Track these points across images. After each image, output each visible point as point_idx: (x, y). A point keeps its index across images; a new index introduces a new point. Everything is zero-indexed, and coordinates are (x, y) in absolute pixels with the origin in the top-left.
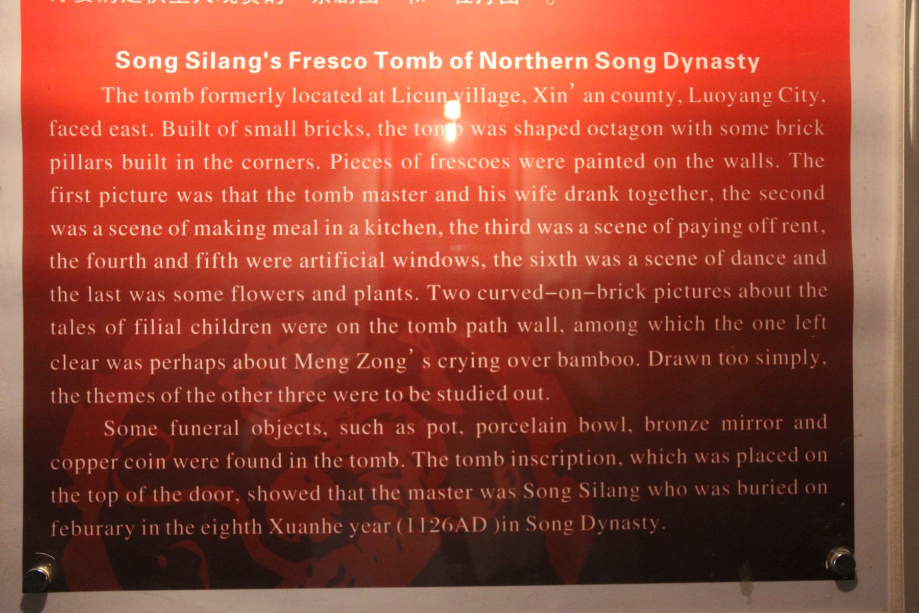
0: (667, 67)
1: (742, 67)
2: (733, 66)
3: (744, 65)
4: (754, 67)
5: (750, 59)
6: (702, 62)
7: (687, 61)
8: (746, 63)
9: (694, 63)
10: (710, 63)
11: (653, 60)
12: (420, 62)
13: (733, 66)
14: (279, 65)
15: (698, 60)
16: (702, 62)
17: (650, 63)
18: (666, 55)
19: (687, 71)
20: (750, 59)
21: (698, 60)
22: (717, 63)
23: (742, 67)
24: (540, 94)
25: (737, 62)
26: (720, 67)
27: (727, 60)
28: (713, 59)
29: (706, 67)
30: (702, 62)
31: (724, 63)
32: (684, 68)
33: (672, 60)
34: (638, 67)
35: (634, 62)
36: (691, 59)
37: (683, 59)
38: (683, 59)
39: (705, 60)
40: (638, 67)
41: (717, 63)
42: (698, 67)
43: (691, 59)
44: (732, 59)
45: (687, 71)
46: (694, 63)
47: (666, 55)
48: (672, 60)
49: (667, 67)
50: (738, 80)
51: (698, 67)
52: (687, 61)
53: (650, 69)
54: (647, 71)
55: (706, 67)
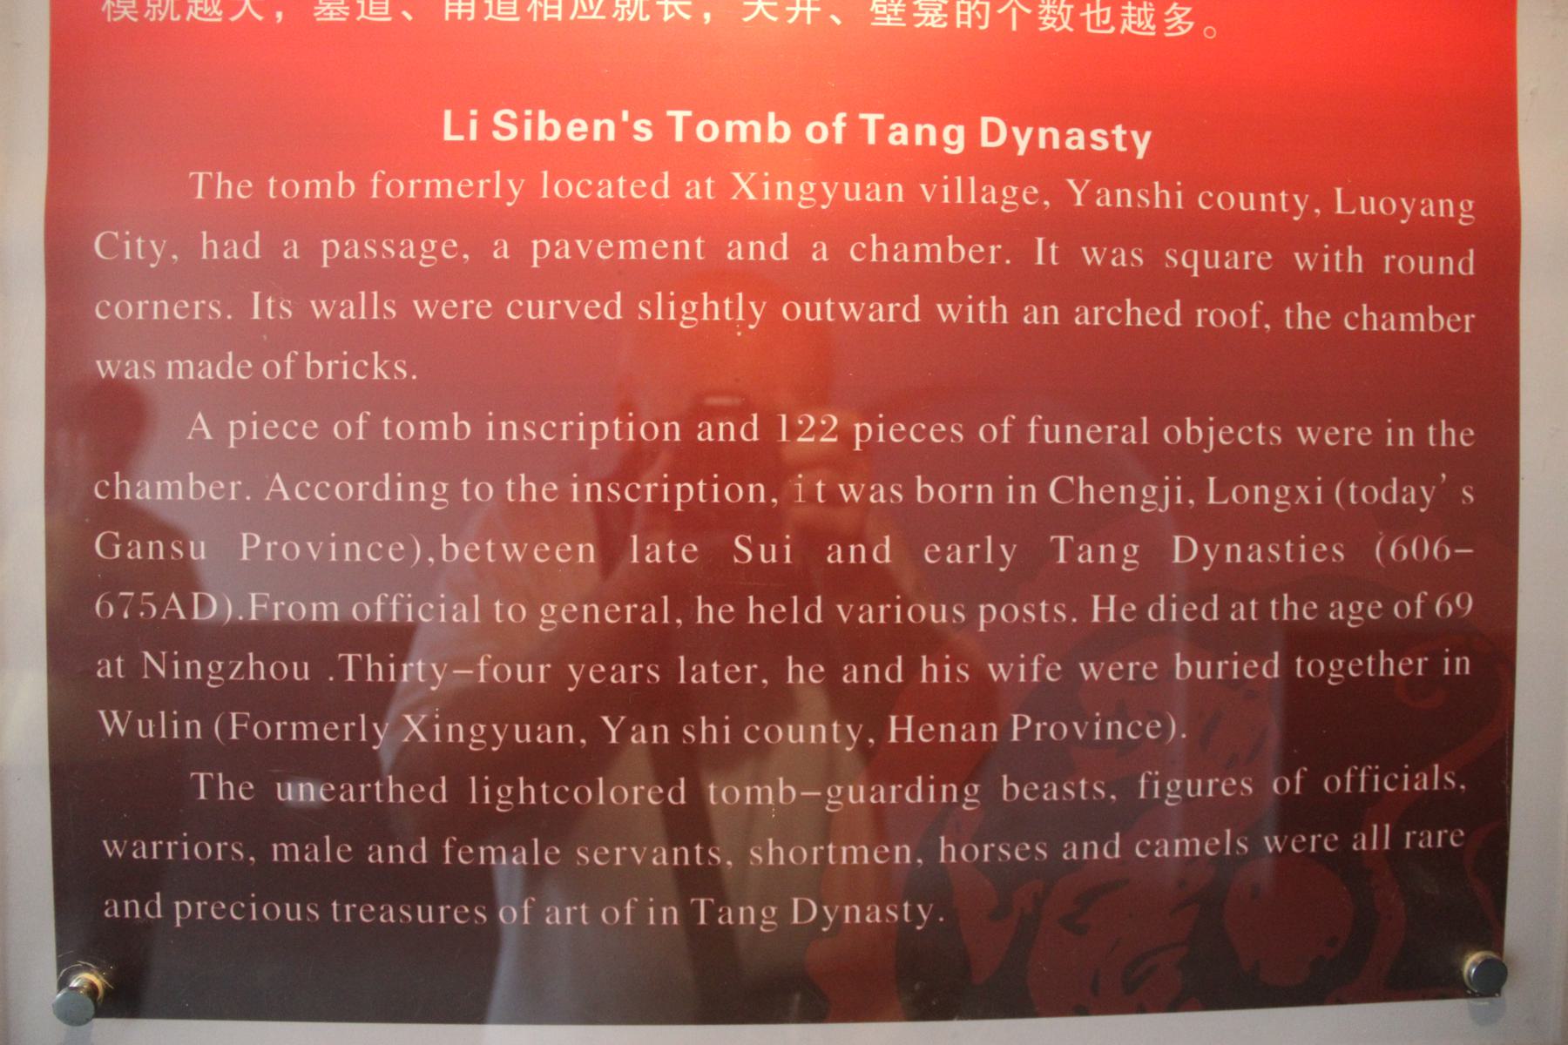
0: (985, 143)
1: (1120, 147)
2: (1105, 145)
3: (1124, 144)
4: (1141, 148)
5: (1135, 134)
6: (1049, 137)
7: (1023, 134)
8: (1128, 140)
9: (1035, 136)
10: (1063, 138)
11: (960, 130)
12: (750, 130)
13: (1105, 145)
14: (649, 135)
15: (1042, 132)
16: (1049, 137)
17: (953, 135)
18: (985, 121)
19: (1021, 152)
20: (1135, 134)
21: (1042, 132)
22: (1076, 140)
23: (1120, 147)
24: (744, 185)
25: (1111, 139)
26: (1081, 146)
27: (1094, 135)
28: (1070, 132)
29: (1056, 145)
30: (1047, 135)
31: (1088, 141)
32: (1016, 147)
33: (994, 131)
34: (933, 141)
35: (926, 133)
36: (1029, 131)
37: (1016, 130)
38: (1016, 130)
39: (1055, 133)
40: (933, 141)
41: (1076, 140)
42: (1042, 145)
43: (1029, 131)
44: (1104, 133)
45: (1021, 152)
46: (1035, 136)
47: (985, 121)
48: (994, 131)
49: (985, 143)
50: (1114, 168)
51: (1042, 145)
52: (1023, 134)
53: (954, 147)
54: (948, 150)
55: (1056, 145)
